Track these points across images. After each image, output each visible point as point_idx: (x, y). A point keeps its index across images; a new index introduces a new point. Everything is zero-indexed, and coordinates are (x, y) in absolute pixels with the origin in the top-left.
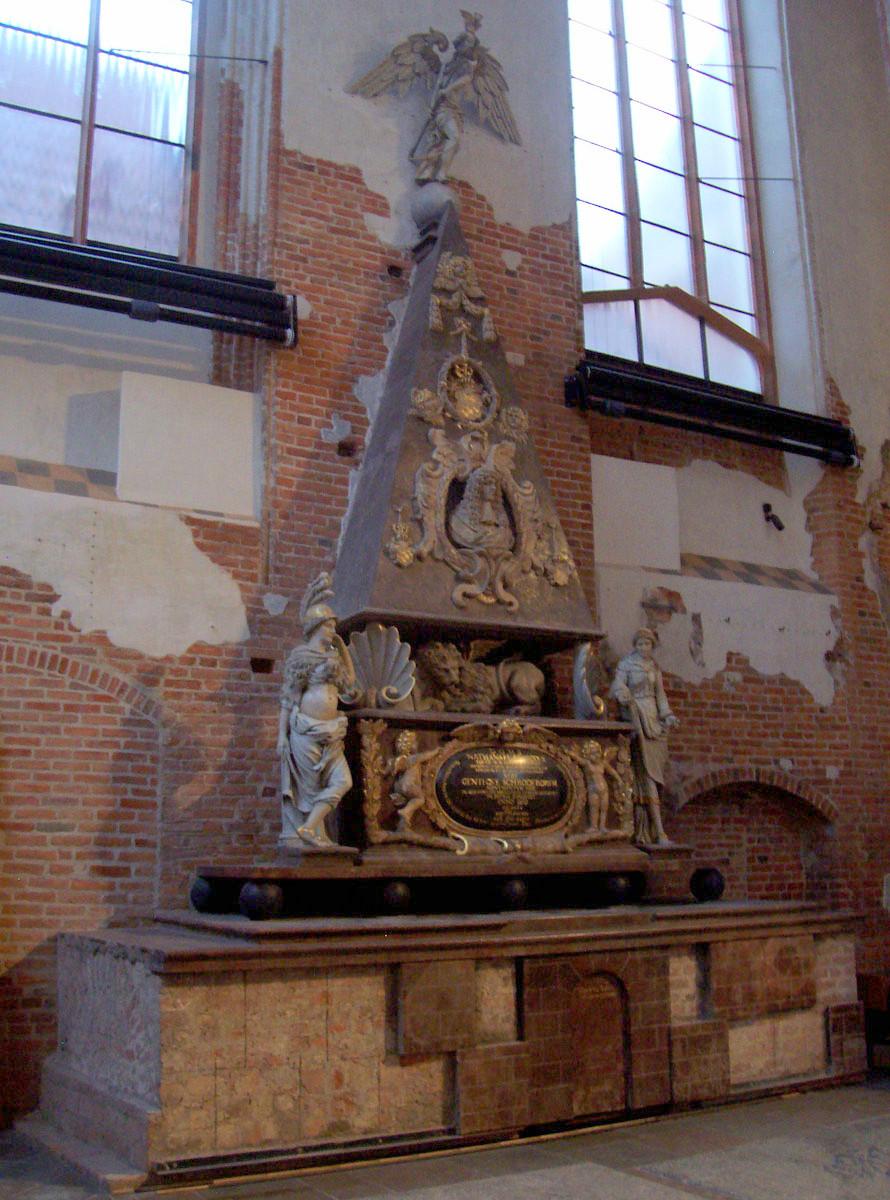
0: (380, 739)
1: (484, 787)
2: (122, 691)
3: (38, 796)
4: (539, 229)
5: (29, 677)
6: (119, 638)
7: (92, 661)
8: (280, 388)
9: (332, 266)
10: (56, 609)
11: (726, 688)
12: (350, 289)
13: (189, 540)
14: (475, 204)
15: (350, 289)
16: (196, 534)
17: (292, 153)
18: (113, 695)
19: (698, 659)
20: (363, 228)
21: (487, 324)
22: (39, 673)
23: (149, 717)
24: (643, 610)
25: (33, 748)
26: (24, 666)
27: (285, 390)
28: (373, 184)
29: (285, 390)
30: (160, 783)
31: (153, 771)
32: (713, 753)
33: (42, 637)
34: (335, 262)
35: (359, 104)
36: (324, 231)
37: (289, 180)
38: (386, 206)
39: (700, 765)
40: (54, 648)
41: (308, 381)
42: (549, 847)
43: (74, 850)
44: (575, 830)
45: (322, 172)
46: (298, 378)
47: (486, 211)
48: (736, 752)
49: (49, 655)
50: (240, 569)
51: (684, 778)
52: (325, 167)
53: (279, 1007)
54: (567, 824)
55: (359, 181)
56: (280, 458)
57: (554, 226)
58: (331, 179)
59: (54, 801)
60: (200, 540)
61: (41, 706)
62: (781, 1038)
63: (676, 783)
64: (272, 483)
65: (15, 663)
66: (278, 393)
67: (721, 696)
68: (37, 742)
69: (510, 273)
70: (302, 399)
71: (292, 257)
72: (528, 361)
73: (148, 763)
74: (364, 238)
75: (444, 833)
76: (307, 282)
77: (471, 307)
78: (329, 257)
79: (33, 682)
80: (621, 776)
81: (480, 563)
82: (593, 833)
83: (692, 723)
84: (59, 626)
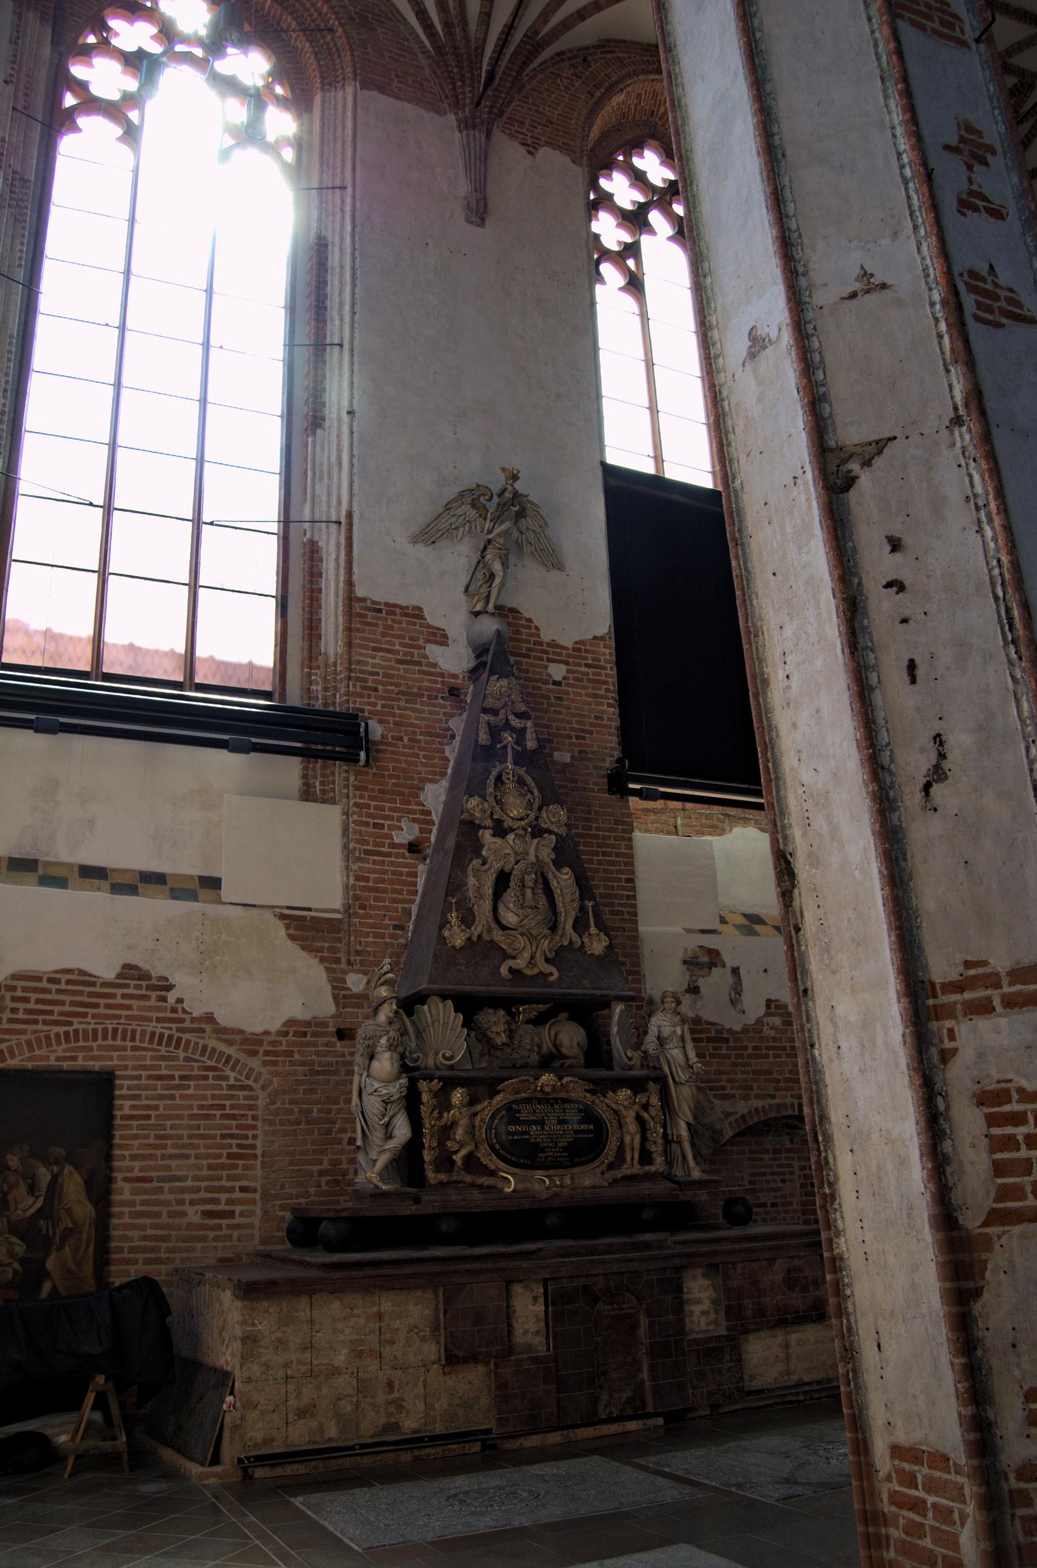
0: (435, 1095)
1: (527, 1133)
2: (227, 1062)
3: (158, 1153)
4: (582, 642)
5: (149, 1054)
6: (224, 1019)
7: (203, 1038)
8: (358, 800)
9: (399, 692)
10: (172, 997)
11: (768, 1032)
12: (414, 710)
13: (283, 932)
14: (523, 626)
15: (414, 710)
16: (288, 927)
17: (363, 600)
18: (220, 1066)
19: (739, 1006)
20: (426, 657)
21: (530, 735)
22: (158, 1051)
23: (250, 1083)
24: (685, 967)
25: (153, 1113)
26: (146, 1045)
27: (362, 801)
28: (432, 619)
29: (362, 801)
30: (260, 1138)
31: (254, 1127)
32: (756, 1091)
33: (159, 1020)
34: (403, 688)
35: (421, 550)
36: (393, 663)
37: (360, 623)
38: (445, 636)
39: (742, 1102)
40: (170, 1029)
41: (380, 791)
42: (589, 1179)
43: (188, 1197)
44: (611, 1167)
45: (389, 613)
46: (373, 790)
47: (533, 631)
48: (777, 1089)
49: (166, 1036)
50: (326, 954)
51: (729, 1115)
52: (392, 608)
53: (339, 1326)
54: (603, 1162)
55: (422, 617)
56: (359, 859)
57: (595, 638)
58: (398, 617)
59: (171, 1157)
60: (291, 932)
61: (159, 1078)
63: (722, 1120)
64: (352, 881)
65: (137, 1043)
66: (356, 805)
67: (762, 1039)
68: (156, 1108)
69: (556, 683)
70: (376, 808)
71: (365, 688)
72: (573, 758)
73: (250, 1122)
74: (427, 665)
75: (493, 1174)
76: (379, 708)
77: (516, 723)
78: (397, 685)
79: (152, 1058)
80: (653, 1118)
81: (522, 941)
82: (626, 1170)
83: (734, 1065)
84: (174, 1010)
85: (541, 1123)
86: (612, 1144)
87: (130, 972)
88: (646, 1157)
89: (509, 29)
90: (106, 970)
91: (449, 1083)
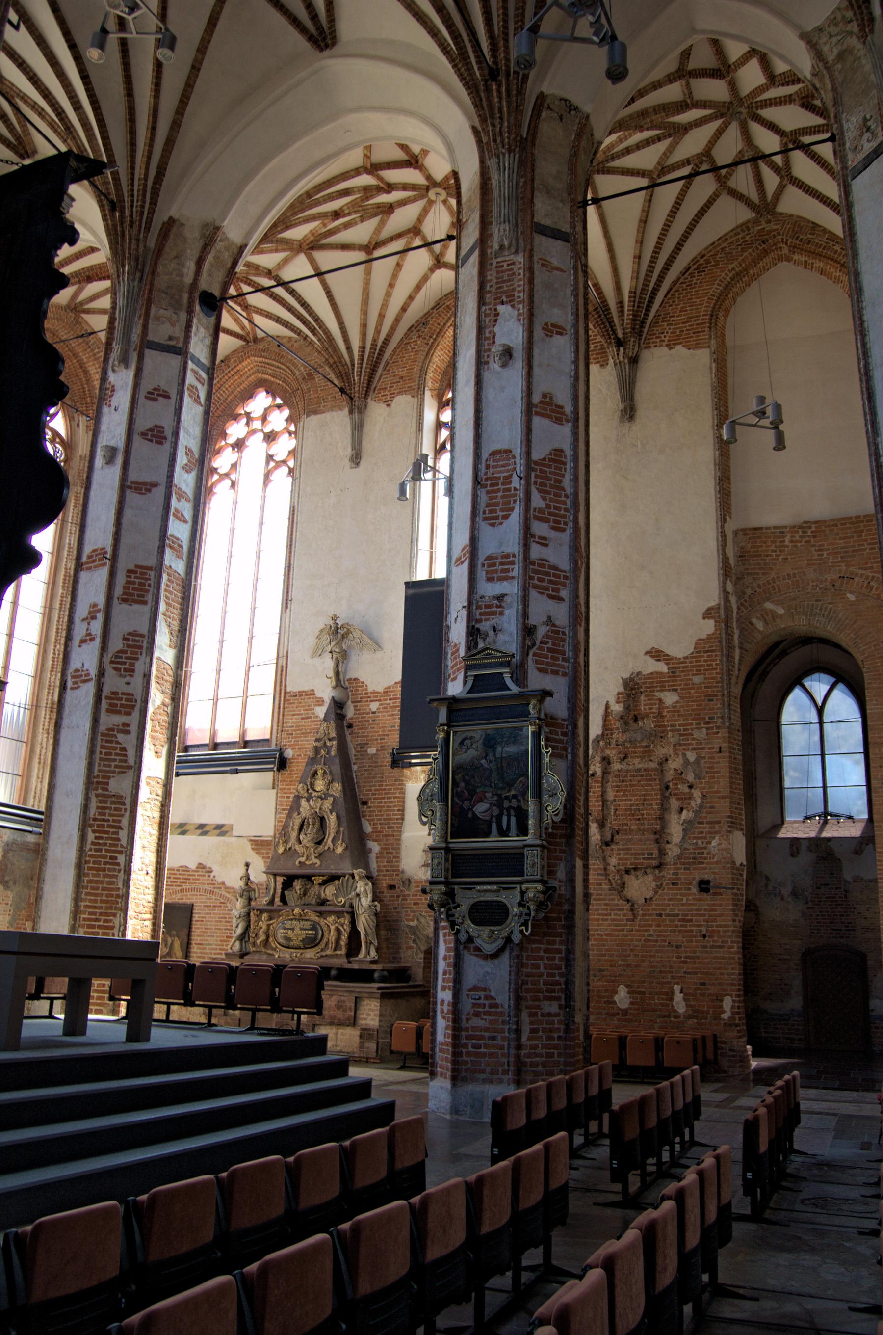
4: (389, 687)
6: (228, 884)
10: (212, 875)
28: (318, 695)
44: (322, 950)
62: (340, 1036)
82: (329, 952)
85: (293, 929)
86: (325, 940)
87: (201, 866)
88: (337, 946)
89: (362, 348)
90: (193, 866)
91: (261, 911)
